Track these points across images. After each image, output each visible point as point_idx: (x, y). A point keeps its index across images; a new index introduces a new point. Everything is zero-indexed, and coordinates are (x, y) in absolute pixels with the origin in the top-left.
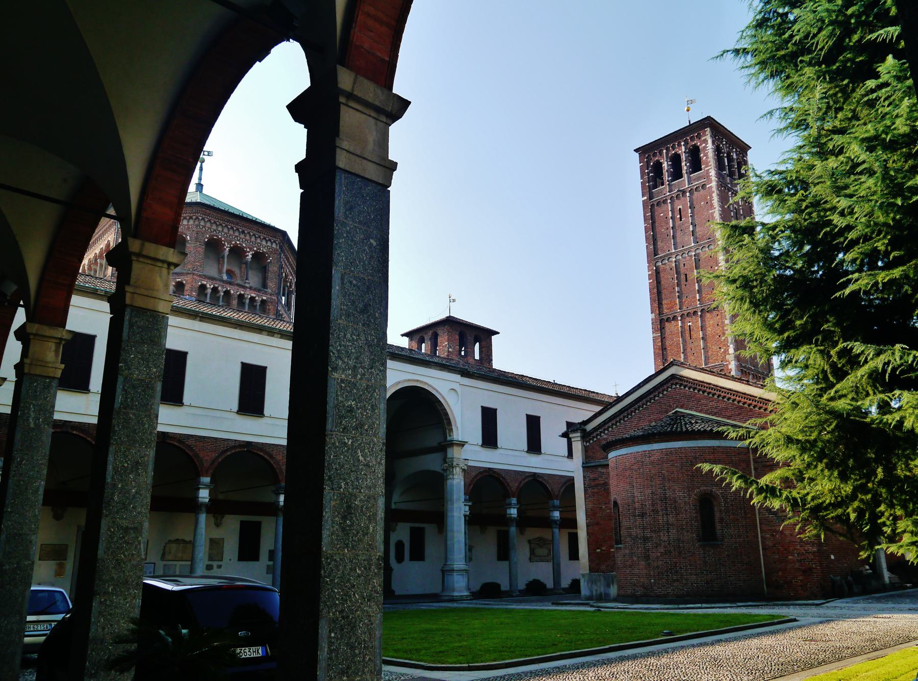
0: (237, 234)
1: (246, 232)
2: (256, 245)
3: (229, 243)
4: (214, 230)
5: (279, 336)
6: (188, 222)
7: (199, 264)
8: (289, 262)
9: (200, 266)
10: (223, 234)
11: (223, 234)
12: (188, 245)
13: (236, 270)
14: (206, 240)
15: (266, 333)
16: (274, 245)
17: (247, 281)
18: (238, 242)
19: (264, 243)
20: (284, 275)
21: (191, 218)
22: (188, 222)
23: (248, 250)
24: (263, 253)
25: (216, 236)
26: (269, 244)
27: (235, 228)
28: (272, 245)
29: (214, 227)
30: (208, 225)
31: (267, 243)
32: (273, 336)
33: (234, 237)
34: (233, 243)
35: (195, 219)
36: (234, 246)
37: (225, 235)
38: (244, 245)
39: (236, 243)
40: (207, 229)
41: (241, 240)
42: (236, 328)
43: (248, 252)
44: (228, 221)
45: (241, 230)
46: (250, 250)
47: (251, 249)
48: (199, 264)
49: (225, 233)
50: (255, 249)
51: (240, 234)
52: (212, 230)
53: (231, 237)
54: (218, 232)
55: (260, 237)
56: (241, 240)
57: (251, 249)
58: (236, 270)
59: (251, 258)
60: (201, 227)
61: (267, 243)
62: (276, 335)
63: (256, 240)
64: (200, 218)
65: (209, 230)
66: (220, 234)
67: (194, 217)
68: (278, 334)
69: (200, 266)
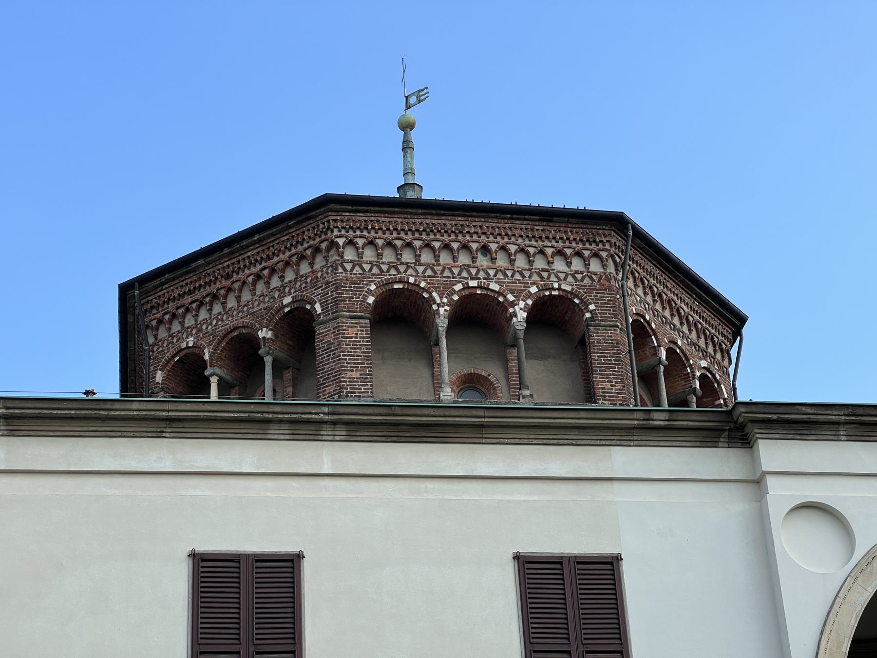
0: (464, 259)
1: (493, 247)
2: (535, 277)
3: (446, 289)
4: (391, 266)
5: (341, 432)
6: (312, 264)
7: (358, 375)
8: (676, 311)
9: (364, 380)
10: (421, 269)
11: (421, 269)
12: (320, 330)
13: (492, 371)
14: (371, 300)
15: (285, 429)
16: (595, 266)
17: (527, 392)
18: (473, 283)
19: (559, 265)
20: (663, 354)
21: (317, 250)
22: (312, 264)
23: (511, 297)
24: (565, 299)
25: (400, 282)
26: (577, 264)
27: (455, 245)
28: (587, 265)
29: (388, 256)
30: (369, 254)
31: (569, 264)
32: (315, 437)
33: (456, 271)
34: (458, 287)
35: (328, 249)
36: (462, 298)
37: (429, 272)
38: (495, 286)
39: (466, 287)
40: (367, 267)
41: (482, 274)
42: (159, 435)
43: (513, 304)
44: (428, 230)
45: (474, 246)
46: (517, 297)
47: (517, 294)
48: (358, 375)
49: (428, 266)
50: (534, 290)
51: (474, 259)
52: (385, 267)
53: (447, 273)
54: (402, 268)
55: (541, 252)
56: (482, 274)
57: (517, 294)
58: (492, 371)
59: (528, 320)
60: (348, 267)
61: (569, 264)
62: (326, 431)
63: (531, 263)
64: (341, 241)
65: (375, 270)
66: (410, 271)
67: (324, 246)
68: (334, 423)
69: (364, 380)
